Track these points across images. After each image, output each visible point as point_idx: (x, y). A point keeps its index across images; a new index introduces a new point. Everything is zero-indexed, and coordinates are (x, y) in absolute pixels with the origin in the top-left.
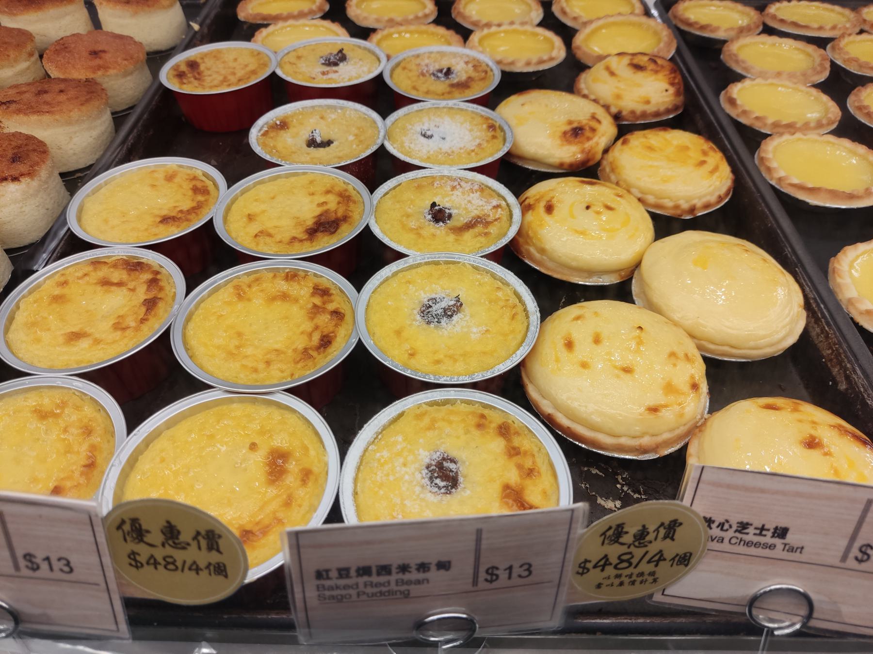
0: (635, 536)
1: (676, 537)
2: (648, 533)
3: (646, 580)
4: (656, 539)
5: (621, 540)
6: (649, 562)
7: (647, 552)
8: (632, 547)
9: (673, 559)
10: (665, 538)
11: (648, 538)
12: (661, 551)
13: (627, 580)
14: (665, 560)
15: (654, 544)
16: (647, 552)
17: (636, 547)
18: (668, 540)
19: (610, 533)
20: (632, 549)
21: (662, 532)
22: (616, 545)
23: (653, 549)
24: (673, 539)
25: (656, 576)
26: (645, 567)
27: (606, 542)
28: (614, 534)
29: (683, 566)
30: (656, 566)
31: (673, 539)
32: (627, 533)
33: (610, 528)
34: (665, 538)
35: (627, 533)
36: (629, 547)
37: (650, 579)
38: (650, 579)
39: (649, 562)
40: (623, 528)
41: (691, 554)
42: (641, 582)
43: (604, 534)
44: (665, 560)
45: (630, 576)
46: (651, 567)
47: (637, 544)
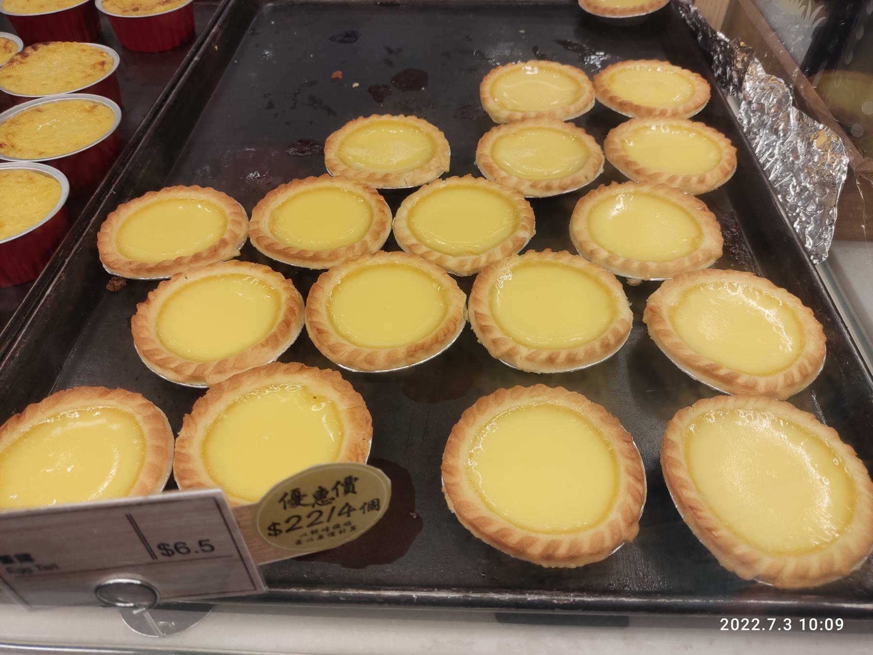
0: (315, 497)
1: (356, 489)
2: (327, 492)
3: (344, 530)
4: (337, 495)
5: (302, 502)
6: (340, 514)
7: (333, 508)
8: (316, 506)
9: (363, 508)
10: (346, 492)
11: (329, 496)
12: (347, 504)
13: (325, 534)
14: (354, 510)
15: (337, 499)
16: (333, 508)
17: (319, 505)
18: (350, 495)
19: (288, 498)
20: (317, 507)
21: (341, 489)
22: (299, 507)
23: (339, 503)
24: (354, 492)
25: (353, 524)
26: (336, 519)
27: (287, 506)
28: (292, 498)
29: (375, 511)
30: (349, 516)
31: (354, 492)
32: (305, 495)
33: (286, 494)
34: (346, 492)
35: (305, 495)
36: (313, 506)
37: (348, 528)
38: (348, 528)
39: (340, 514)
40: (299, 493)
41: (378, 500)
42: (340, 532)
43: (282, 500)
44: (354, 510)
45: (327, 529)
46: (344, 519)
47: (320, 502)
